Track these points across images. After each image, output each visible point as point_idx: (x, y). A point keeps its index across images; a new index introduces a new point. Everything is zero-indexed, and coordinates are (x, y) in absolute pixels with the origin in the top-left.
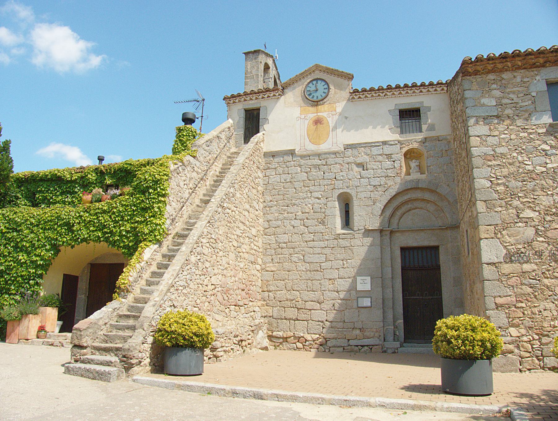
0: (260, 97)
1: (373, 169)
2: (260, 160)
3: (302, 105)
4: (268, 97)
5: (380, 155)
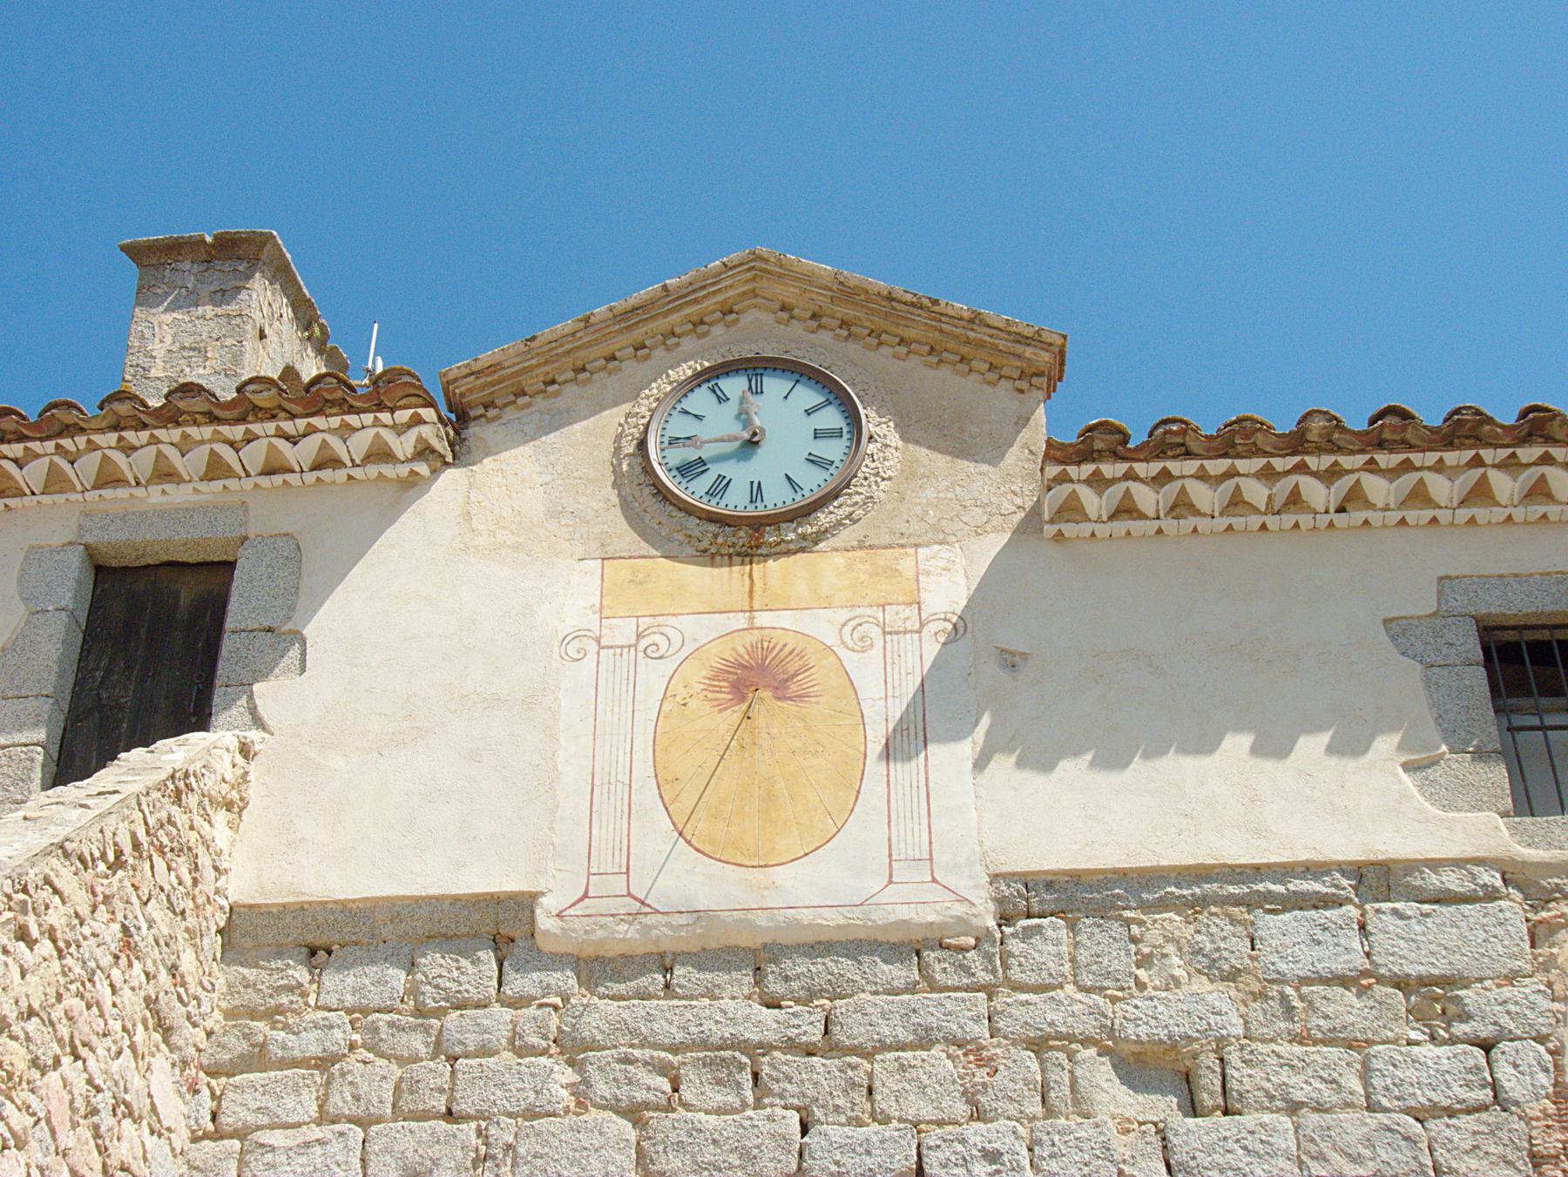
0: (255, 454)
1: (1293, 1108)
2: (188, 962)
3: (616, 547)
4: (326, 461)
5: (1343, 981)
